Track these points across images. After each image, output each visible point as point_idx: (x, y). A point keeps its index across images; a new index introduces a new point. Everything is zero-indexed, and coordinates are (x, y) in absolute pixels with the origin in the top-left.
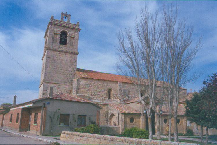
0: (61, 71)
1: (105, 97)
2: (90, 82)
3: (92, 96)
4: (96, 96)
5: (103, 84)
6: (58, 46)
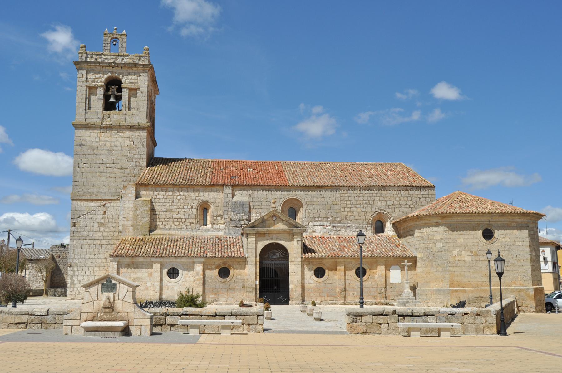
0: (110, 170)
1: (193, 223)
2: (156, 193)
3: (161, 223)
4: (171, 223)
5: (186, 194)
6: (99, 116)
